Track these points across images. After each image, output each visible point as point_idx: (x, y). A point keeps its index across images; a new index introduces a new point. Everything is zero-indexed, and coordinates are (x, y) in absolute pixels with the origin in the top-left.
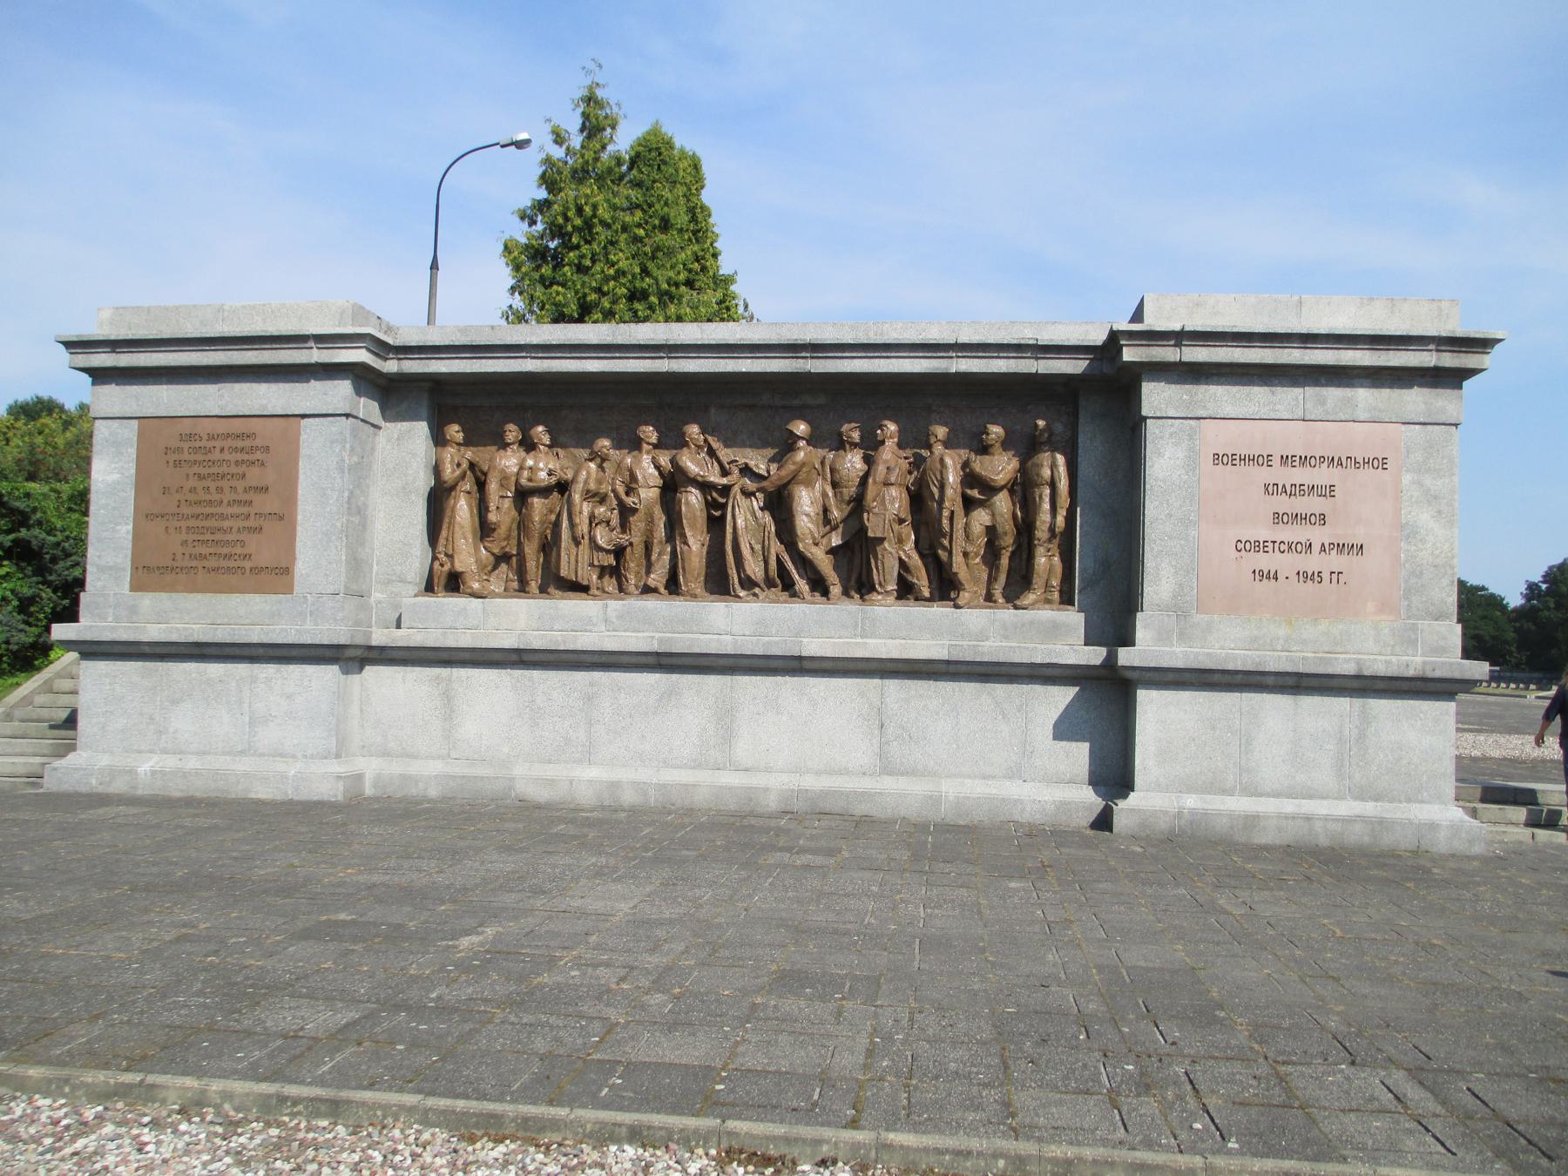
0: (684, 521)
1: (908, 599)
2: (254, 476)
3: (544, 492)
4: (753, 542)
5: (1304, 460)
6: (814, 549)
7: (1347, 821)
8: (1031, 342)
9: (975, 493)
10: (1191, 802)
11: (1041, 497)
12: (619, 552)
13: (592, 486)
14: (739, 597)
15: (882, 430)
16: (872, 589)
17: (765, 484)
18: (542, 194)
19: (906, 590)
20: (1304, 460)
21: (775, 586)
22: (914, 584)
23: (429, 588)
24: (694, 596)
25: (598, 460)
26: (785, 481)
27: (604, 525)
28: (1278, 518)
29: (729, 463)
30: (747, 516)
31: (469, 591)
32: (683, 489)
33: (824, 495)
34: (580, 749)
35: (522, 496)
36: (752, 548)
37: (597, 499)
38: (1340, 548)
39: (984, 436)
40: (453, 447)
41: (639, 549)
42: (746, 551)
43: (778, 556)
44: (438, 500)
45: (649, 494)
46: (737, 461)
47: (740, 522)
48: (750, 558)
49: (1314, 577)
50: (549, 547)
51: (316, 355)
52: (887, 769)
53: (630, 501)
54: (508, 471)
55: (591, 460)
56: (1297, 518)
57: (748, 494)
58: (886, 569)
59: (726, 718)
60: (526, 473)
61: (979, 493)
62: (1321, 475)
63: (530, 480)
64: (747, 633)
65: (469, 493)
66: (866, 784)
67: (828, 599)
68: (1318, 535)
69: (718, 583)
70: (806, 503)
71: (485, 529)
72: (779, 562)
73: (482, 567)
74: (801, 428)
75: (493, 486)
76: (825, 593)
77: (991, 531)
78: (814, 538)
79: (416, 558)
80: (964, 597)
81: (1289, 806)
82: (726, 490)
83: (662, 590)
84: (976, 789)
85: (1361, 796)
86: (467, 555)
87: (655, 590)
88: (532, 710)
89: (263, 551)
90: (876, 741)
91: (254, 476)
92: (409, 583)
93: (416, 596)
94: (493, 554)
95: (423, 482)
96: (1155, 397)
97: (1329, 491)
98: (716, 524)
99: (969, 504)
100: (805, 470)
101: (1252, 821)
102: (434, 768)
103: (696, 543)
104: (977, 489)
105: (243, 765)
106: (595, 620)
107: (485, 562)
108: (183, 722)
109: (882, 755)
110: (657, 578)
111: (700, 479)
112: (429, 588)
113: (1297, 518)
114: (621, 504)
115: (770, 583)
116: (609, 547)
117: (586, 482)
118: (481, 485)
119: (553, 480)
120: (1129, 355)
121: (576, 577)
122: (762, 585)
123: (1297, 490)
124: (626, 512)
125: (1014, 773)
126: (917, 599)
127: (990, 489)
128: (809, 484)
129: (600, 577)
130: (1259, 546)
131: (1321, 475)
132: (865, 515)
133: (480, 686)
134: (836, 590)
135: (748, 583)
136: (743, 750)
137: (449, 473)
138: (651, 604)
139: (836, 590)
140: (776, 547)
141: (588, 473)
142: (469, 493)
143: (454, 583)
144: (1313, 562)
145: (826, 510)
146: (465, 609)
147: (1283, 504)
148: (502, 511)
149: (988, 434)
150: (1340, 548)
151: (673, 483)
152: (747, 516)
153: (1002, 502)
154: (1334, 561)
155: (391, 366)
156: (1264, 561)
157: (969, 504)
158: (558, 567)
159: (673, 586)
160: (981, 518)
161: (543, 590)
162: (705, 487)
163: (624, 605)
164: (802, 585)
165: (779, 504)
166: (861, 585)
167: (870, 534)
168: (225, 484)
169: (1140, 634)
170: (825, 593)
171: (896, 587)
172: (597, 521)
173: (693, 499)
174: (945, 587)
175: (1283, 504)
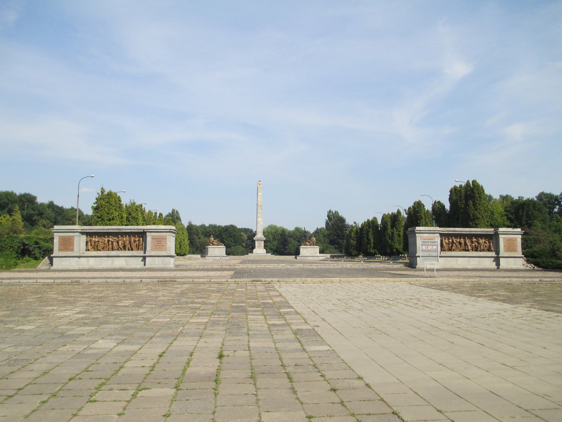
2: (70, 241)
3: (97, 242)
5: (159, 239)
7: (161, 267)
10: (150, 266)
12: (104, 247)
18: (96, 201)
19: (129, 250)
20: (159, 239)
23: (86, 250)
24: (110, 251)
28: (157, 243)
30: (115, 244)
35: (95, 242)
38: (162, 246)
42: (115, 247)
44: (87, 243)
45: (106, 242)
49: (160, 248)
50: (97, 247)
51: (76, 231)
52: (127, 265)
56: (159, 243)
57: (115, 242)
58: (127, 248)
59: (113, 261)
62: (161, 240)
66: (125, 266)
68: (160, 245)
69: (113, 250)
70: (120, 242)
71: (91, 245)
75: (92, 241)
77: (136, 244)
79: (85, 248)
80: (134, 250)
81: (158, 266)
82: (113, 242)
84: (134, 266)
85: (163, 265)
86: (90, 247)
89: (71, 248)
91: (70, 241)
95: (85, 241)
96: (148, 234)
97: (161, 241)
98: (112, 244)
99: (134, 242)
101: (154, 267)
102: (87, 266)
103: (110, 246)
104: (135, 241)
105: (70, 267)
108: (63, 263)
110: (107, 249)
112: (86, 250)
113: (159, 243)
115: (117, 249)
120: (145, 231)
123: (159, 241)
124: (104, 244)
125: (137, 265)
127: (136, 241)
128: (120, 241)
130: (156, 246)
131: (161, 240)
134: (123, 250)
135: (115, 250)
136: (115, 264)
137: (88, 240)
138: (106, 252)
139: (123, 250)
140: (118, 246)
143: (88, 250)
144: (160, 247)
147: (158, 242)
148: (93, 243)
150: (162, 246)
151: (108, 241)
152: (115, 244)
153: (137, 242)
154: (162, 247)
155: (83, 231)
156: (156, 247)
157: (134, 242)
159: (109, 250)
160: (135, 243)
161: (97, 251)
162: (111, 241)
164: (120, 249)
165: (118, 243)
166: (125, 249)
168: (67, 242)
169: (146, 253)
173: (110, 242)
174: (132, 250)
175: (158, 242)
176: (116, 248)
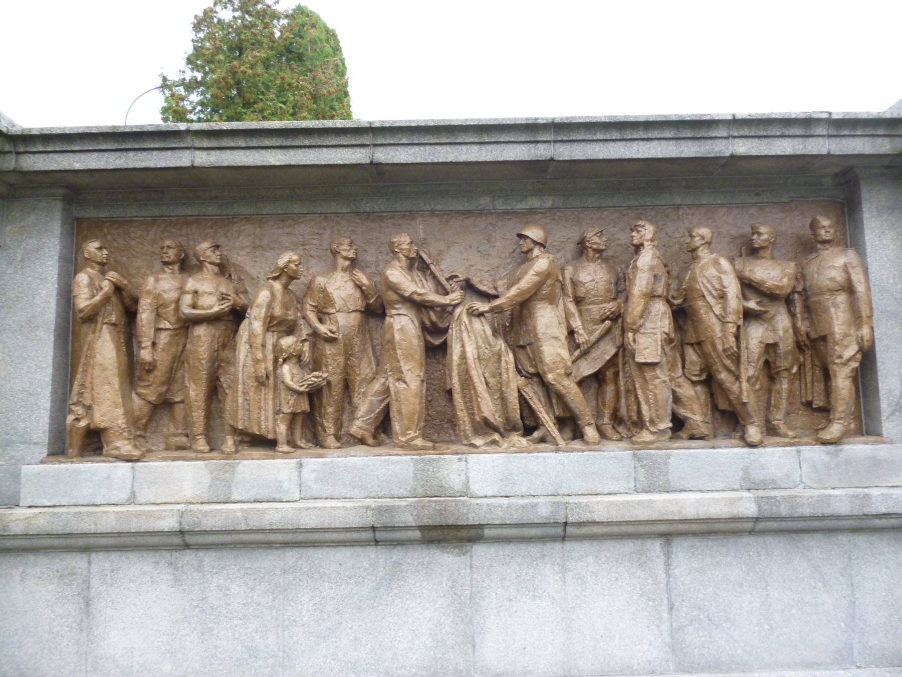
0: (399, 352)
1: (681, 438)
3: (212, 320)
4: (486, 375)
6: (566, 382)
8: (825, 116)
9: (752, 304)
11: (836, 306)
12: (314, 395)
13: (278, 311)
14: (473, 446)
15: (638, 232)
16: (639, 424)
17: (497, 302)
21: (514, 429)
22: (690, 418)
25: (284, 279)
26: (527, 296)
27: (294, 360)
29: (448, 279)
31: (116, 452)
32: (394, 312)
33: (568, 316)
34: (270, 661)
36: (487, 384)
37: (283, 328)
39: (755, 237)
40: (93, 268)
41: (337, 390)
43: (519, 391)
46: (456, 277)
47: (471, 351)
48: (486, 395)
53: (323, 329)
54: (166, 296)
55: (275, 278)
57: (475, 314)
60: (188, 299)
61: (758, 303)
63: (194, 306)
64: (490, 494)
65: (114, 325)
67: (587, 443)
72: (524, 402)
73: (133, 421)
74: (535, 233)
75: (145, 316)
76: (578, 434)
77: (771, 348)
78: (566, 367)
80: (753, 432)
82: (446, 311)
83: (370, 441)
87: (362, 441)
88: (203, 611)
90: (665, 627)
92: (35, 444)
93: (42, 462)
94: (150, 403)
100: (549, 282)
106: (286, 486)
107: (137, 413)
109: (675, 647)
110: (359, 425)
111: (416, 297)
114: (315, 334)
115: (510, 428)
116: (302, 389)
117: (270, 306)
118: (130, 314)
119: (225, 306)
121: (260, 428)
122: (502, 430)
126: (692, 437)
128: (551, 300)
129: (291, 428)
132: (630, 335)
133: (131, 581)
134: (590, 432)
135: (485, 427)
137: (84, 300)
140: (514, 382)
141: (273, 295)
142: (114, 325)
145: (571, 333)
146: (108, 478)
149: (759, 234)
158: (235, 416)
160: (756, 334)
162: (419, 306)
163: (324, 464)
167: (640, 359)
170: (578, 434)
171: (670, 425)
172: (285, 355)
176: (488, 408)
